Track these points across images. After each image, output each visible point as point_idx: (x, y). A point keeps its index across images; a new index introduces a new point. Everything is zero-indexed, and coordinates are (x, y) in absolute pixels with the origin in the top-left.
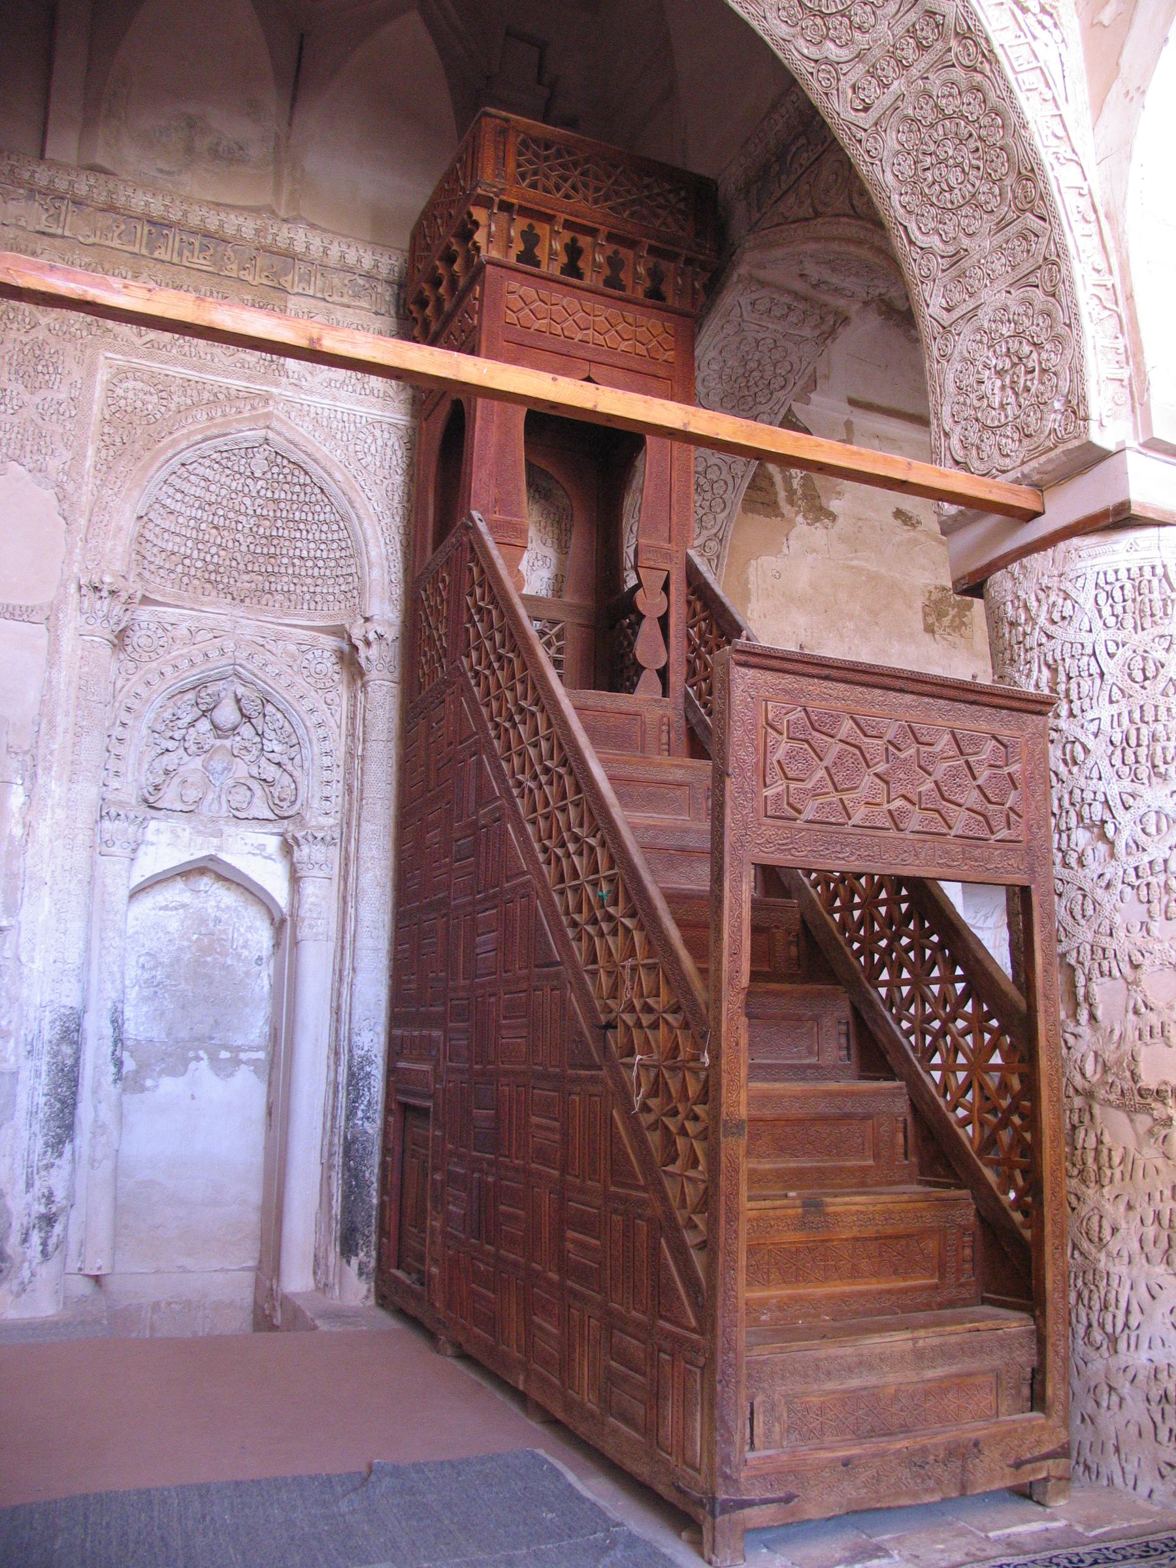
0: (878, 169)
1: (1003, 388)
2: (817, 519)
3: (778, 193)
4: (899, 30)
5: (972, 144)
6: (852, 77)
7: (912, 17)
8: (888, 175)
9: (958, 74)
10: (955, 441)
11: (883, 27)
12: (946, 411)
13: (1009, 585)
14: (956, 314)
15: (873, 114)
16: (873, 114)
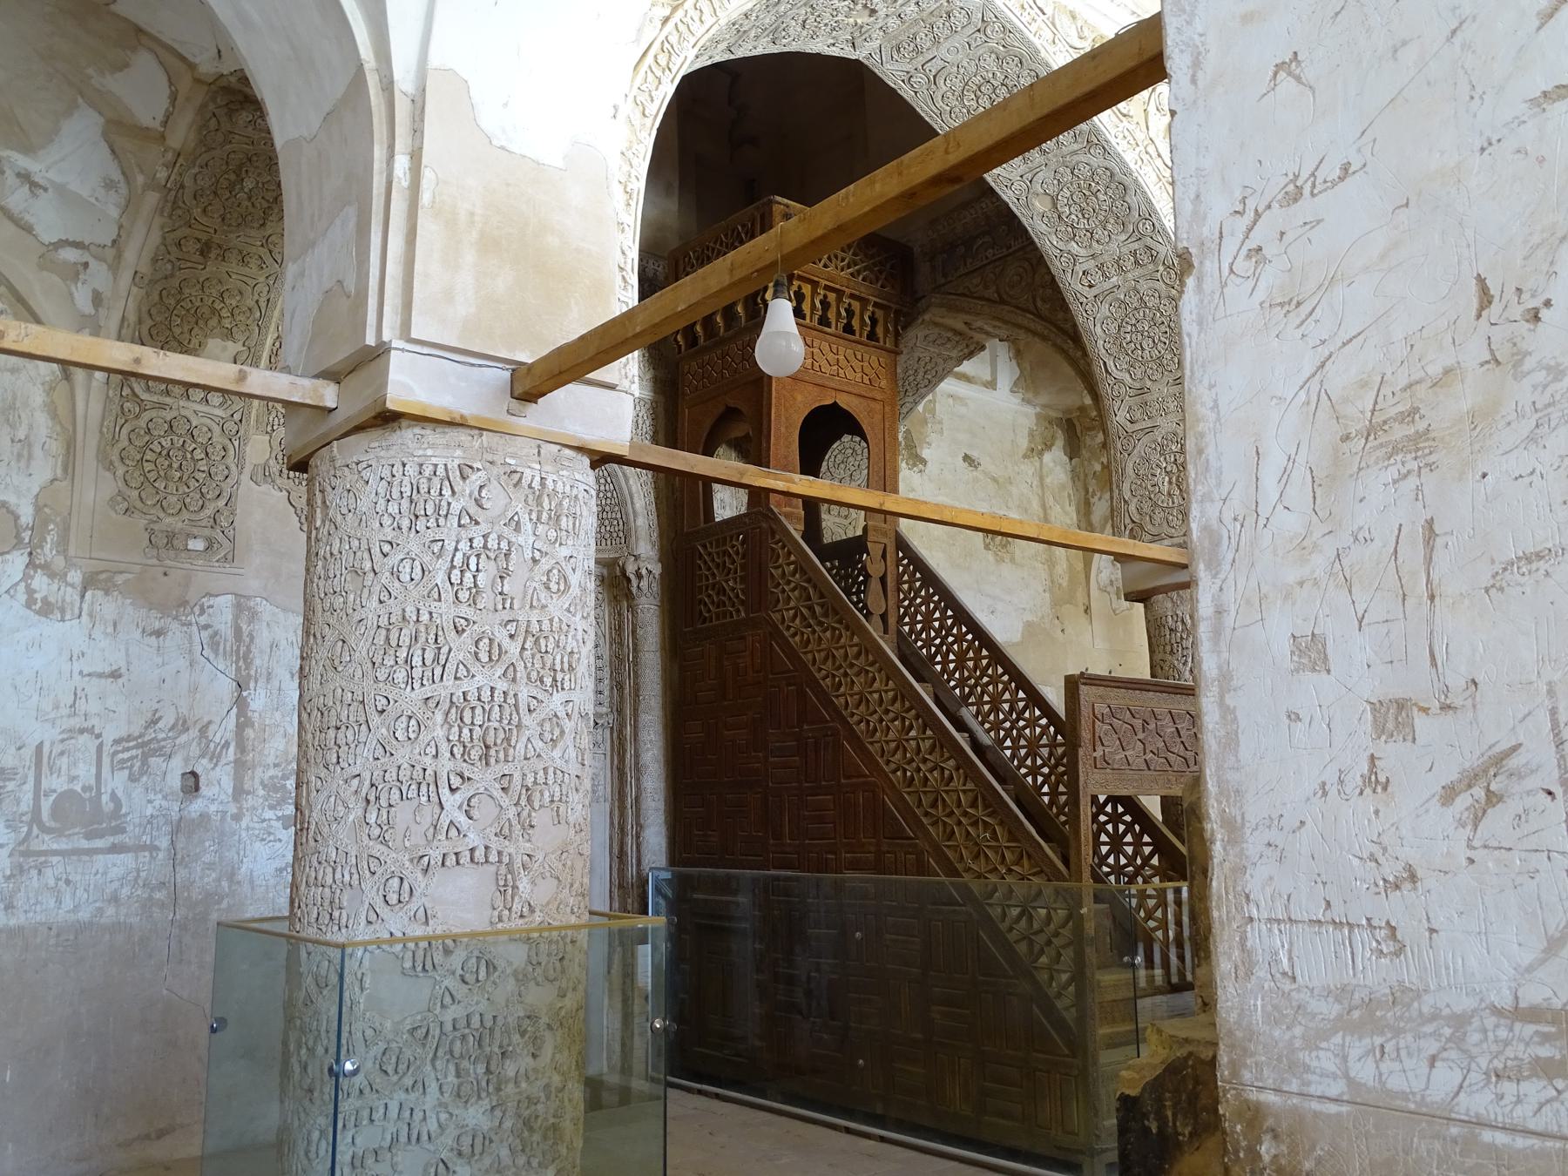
0: (1091, 323)
1: (1170, 483)
2: (915, 465)
3: (962, 271)
4: (1125, 250)
5: (1163, 328)
6: (1085, 267)
7: (1136, 246)
8: (1098, 330)
9: (1160, 285)
10: (1132, 508)
11: (1114, 245)
12: (1126, 487)
13: (1169, 605)
14: (1137, 427)
15: (1094, 291)
16: (1094, 291)
